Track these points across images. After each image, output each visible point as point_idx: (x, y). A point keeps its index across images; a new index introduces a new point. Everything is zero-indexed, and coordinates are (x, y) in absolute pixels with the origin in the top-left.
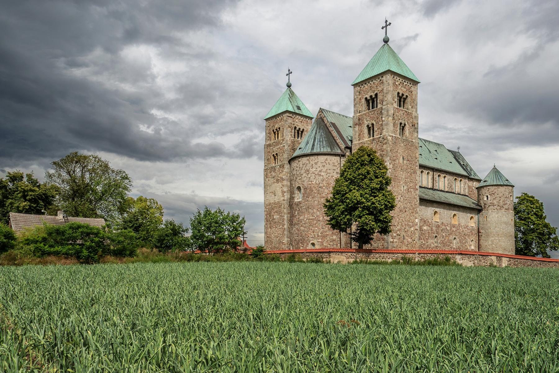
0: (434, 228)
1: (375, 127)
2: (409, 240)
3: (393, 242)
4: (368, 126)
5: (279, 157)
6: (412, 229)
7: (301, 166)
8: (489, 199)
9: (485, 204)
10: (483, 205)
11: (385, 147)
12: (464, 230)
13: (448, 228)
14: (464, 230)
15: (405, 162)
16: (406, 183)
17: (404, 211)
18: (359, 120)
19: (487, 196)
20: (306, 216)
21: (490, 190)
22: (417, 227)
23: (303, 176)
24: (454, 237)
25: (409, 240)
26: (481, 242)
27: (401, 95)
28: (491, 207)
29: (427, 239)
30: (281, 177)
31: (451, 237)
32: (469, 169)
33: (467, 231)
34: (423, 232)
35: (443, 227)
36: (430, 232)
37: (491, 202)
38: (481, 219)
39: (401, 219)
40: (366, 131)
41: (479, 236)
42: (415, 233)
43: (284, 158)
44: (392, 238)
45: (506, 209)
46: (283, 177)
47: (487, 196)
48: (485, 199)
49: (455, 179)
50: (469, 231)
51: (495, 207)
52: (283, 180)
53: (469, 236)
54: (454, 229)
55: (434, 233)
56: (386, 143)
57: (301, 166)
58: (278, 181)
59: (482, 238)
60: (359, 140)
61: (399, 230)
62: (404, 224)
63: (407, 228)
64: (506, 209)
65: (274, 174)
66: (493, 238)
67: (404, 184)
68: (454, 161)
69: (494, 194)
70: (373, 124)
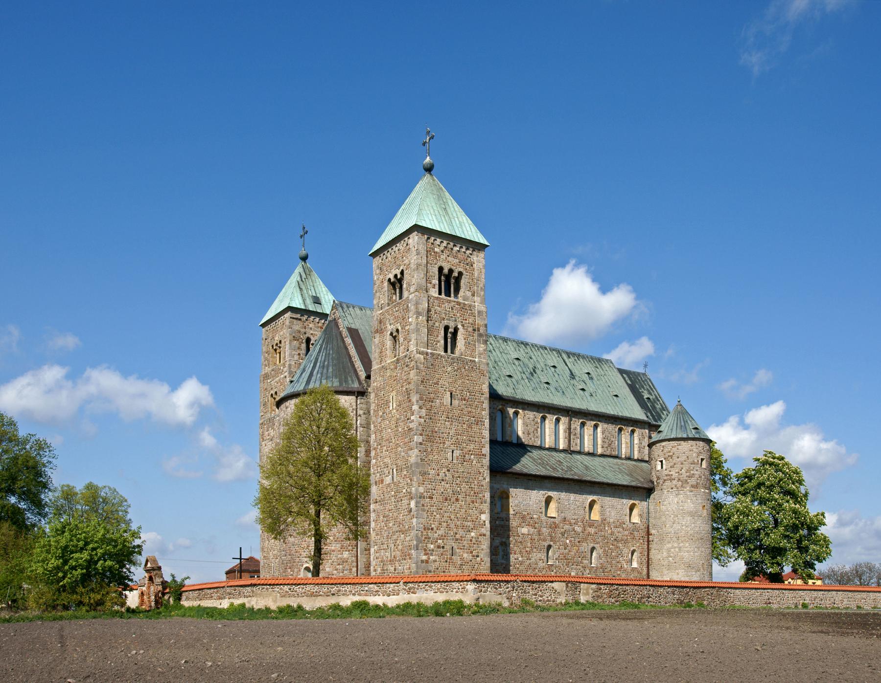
0: (545, 530)
2: (465, 555)
3: (427, 562)
6: (473, 534)
8: (664, 467)
9: (658, 478)
10: (655, 480)
12: (616, 530)
13: (578, 529)
14: (616, 530)
15: (456, 402)
16: (457, 443)
17: (453, 499)
19: (661, 461)
21: (666, 450)
22: (483, 531)
24: (592, 545)
25: (465, 555)
26: (652, 552)
27: (446, 271)
28: (668, 483)
29: (529, 553)
31: (586, 547)
32: (658, 407)
33: (619, 533)
34: (520, 539)
35: (567, 527)
36: (534, 537)
37: (667, 472)
38: (651, 508)
39: (446, 515)
41: (648, 541)
42: (478, 543)
44: (426, 554)
45: (692, 486)
47: (661, 461)
48: (659, 467)
49: (620, 430)
50: (626, 533)
51: (674, 482)
53: (626, 542)
54: (592, 530)
55: (544, 540)
59: (653, 546)
61: (442, 537)
62: (452, 526)
63: (461, 532)
64: (692, 486)
66: (670, 545)
67: (452, 447)
68: (626, 392)
69: (671, 457)
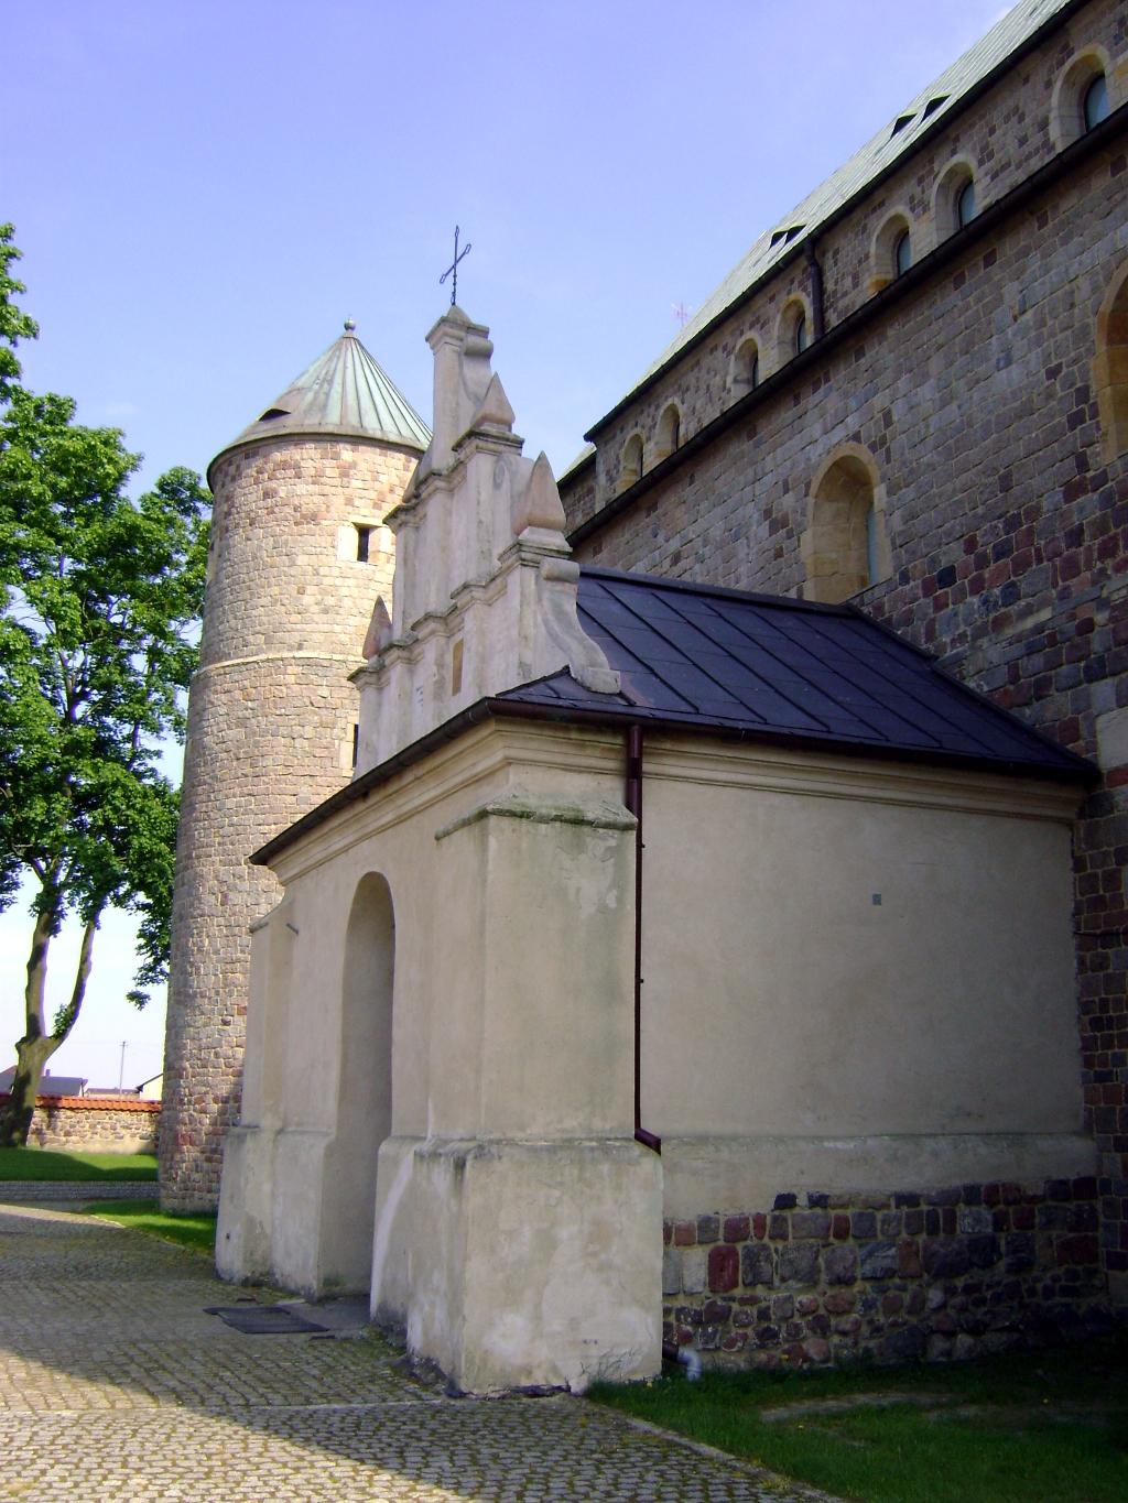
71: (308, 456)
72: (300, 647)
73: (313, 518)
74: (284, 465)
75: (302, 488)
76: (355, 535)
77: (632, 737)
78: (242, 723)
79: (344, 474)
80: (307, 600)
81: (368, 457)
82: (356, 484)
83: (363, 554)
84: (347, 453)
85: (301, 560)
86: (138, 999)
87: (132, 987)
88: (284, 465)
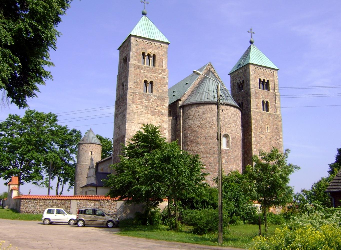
1: (269, 105)
4: (263, 102)
5: (154, 87)
7: (230, 115)
11: (279, 123)
18: (256, 93)
20: (234, 166)
23: (232, 126)
30: (159, 111)
40: (262, 104)
43: (163, 91)
46: (163, 111)
52: (163, 115)
56: (280, 121)
57: (230, 115)
58: (153, 113)
60: (257, 109)
65: (147, 103)
70: (267, 102)
71: (86, 145)
72: (86, 163)
73: (87, 151)
74: (84, 146)
75: (86, 148)
76: (91, 152)
77: (96, 186)
78: (80, 170)
79: (90, 147)
80: (86, 159)
81: (92, 145)
82: (91, 147)
83: (91, 154)
84: (90, 145)
85: (86, 155)
86: (69, 190)
87: (68, 189)
88: (84, 146)
